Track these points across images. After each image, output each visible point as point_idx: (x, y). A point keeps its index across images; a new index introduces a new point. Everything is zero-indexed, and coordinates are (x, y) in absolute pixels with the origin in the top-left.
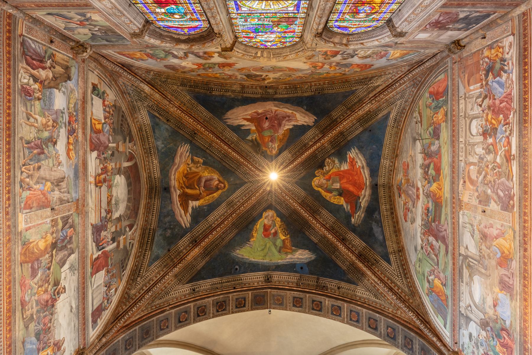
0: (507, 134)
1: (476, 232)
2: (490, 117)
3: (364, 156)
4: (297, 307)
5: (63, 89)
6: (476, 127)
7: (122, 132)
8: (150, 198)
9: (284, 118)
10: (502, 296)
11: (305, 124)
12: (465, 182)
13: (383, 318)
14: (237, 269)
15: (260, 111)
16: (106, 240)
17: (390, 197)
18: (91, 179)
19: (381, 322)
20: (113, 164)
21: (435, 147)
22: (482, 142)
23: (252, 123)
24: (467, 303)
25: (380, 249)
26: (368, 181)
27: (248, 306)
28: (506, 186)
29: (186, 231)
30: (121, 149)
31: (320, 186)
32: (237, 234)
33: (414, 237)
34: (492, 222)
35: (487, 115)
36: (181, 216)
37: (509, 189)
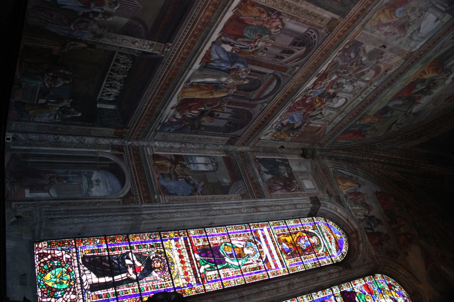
0: (311, 91)
2: (318, 105)
6: (337, 102)
12: (386, 71)
21: (396, 103)
22: (340, 92)
28: (342, 59)
34: (383, 36)
35: (319, 107)
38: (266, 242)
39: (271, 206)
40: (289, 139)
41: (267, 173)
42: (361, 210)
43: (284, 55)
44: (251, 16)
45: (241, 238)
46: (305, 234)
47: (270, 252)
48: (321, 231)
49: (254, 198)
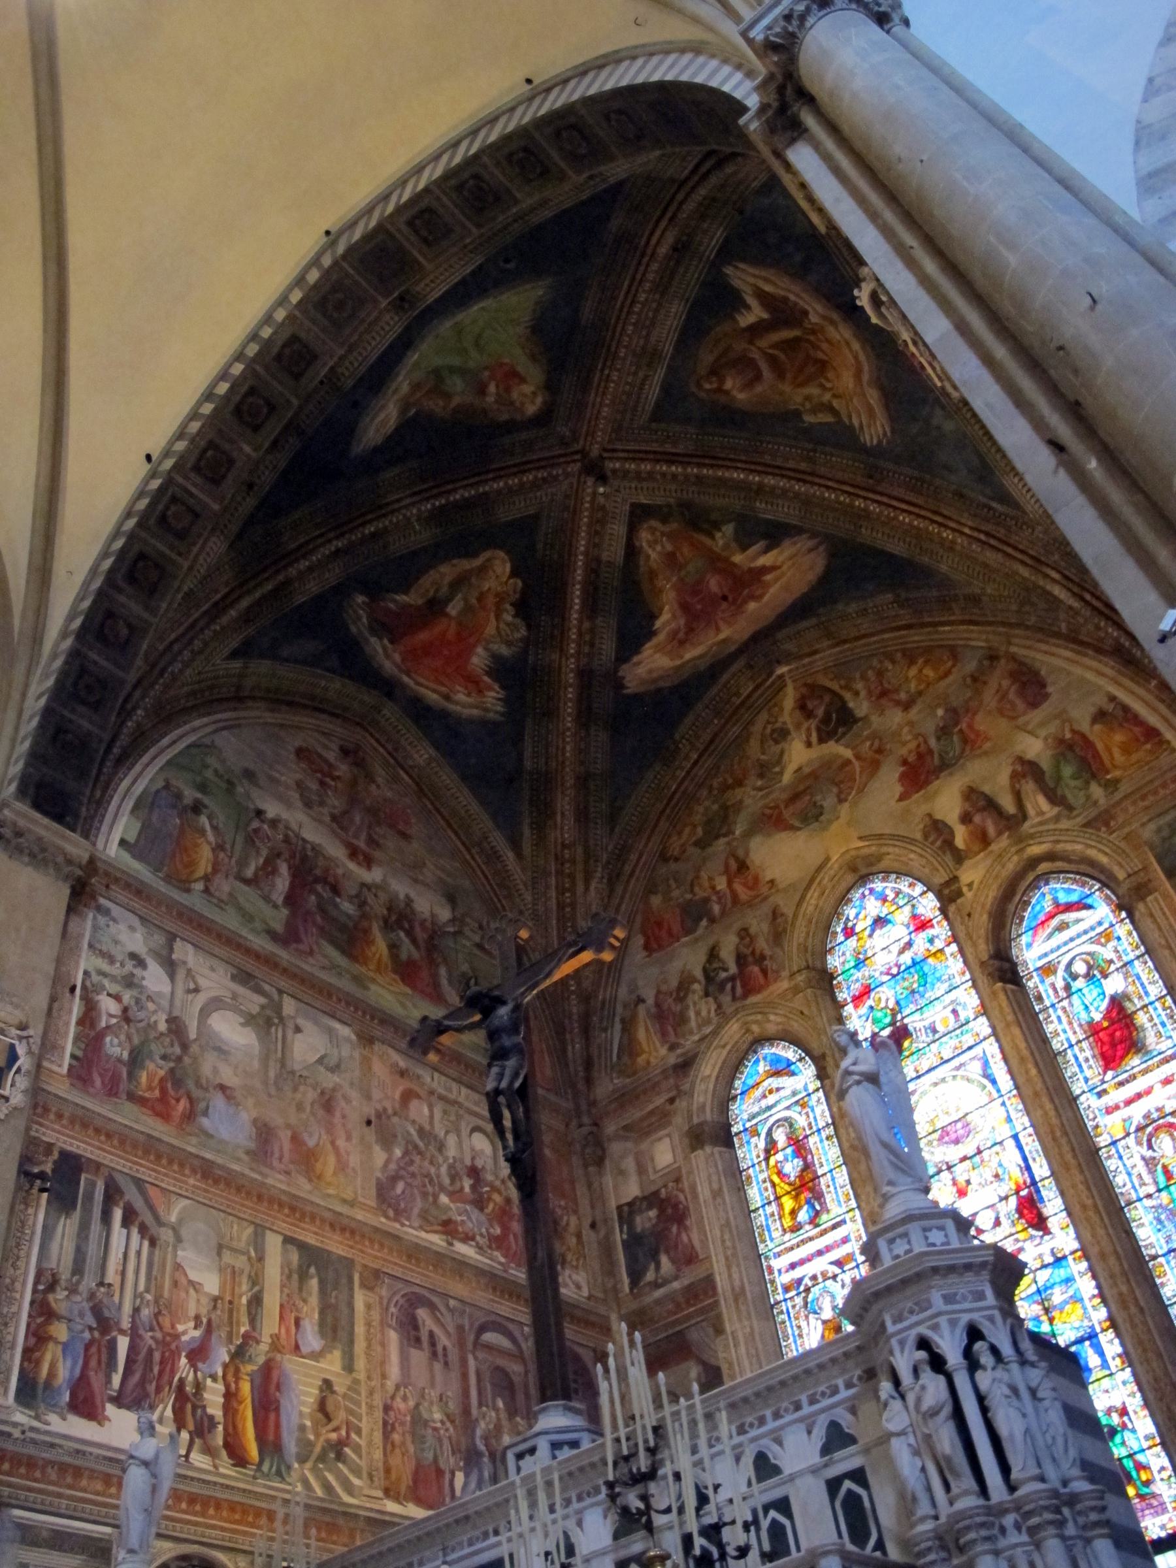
3: (471, 721)
4: (284, 346)
9: (690, 630)
11: (635, 659)
14: (507, 261)
15: (752, 606)
19: (147, 608)
23: (751, 570)
24: (202, 982)
26: (411, 683)
27: (399, 230)
29: (727, 253)
31: (482, 570)
36: (766, 280)
38: (802, 1262)
39: (727, 1259)
40: (573, 1220)
41: (658, 1267)
42: (695, 1004)
45: (803, 1324)
46: (772, 1161)
47: (820, 1253)
48: (758, 1114)
49: (716, 1303)
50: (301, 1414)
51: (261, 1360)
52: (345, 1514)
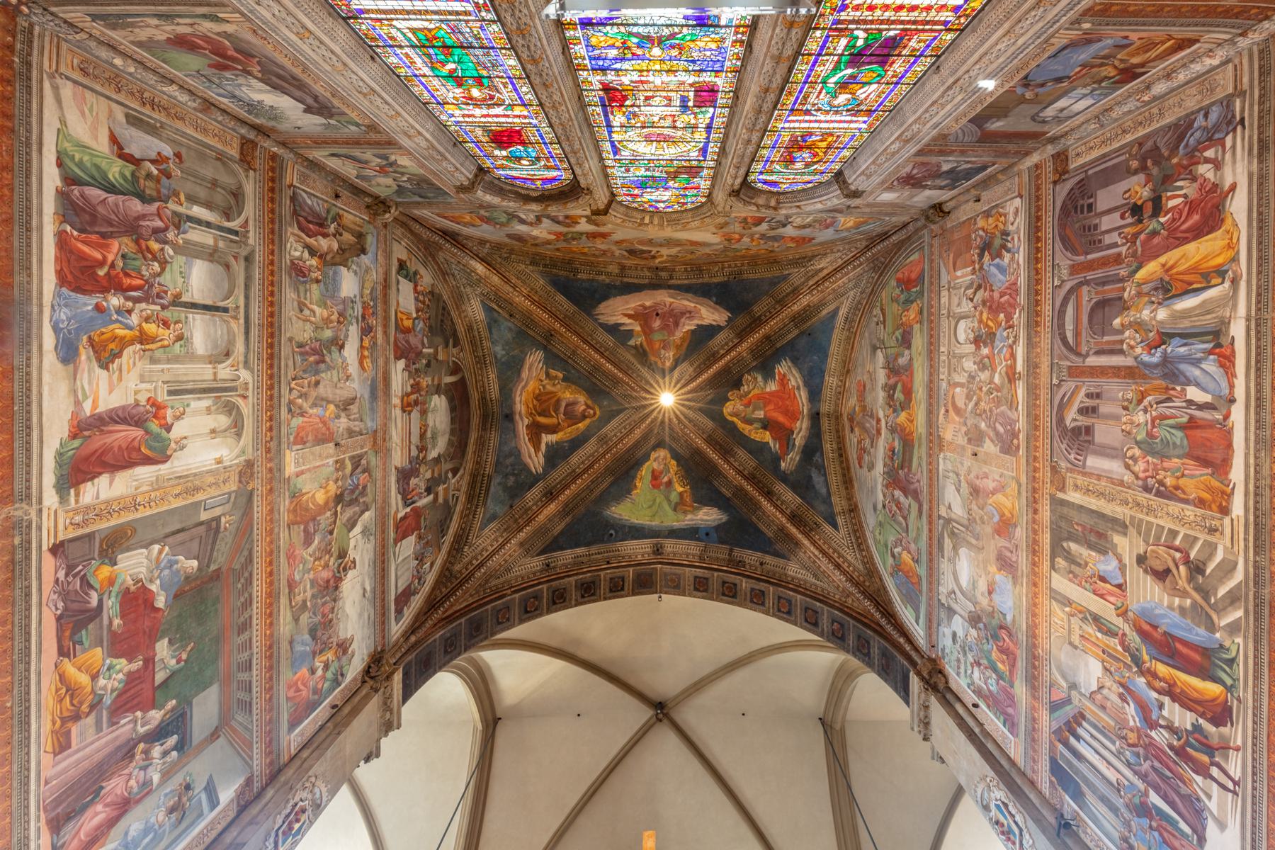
1: (964, 484)
3: (800, 370)
5: (354, 267)
7: (443, 331)
8: (484, 429)
10: (1001, 578)
12: (947, 411)
13: (826, 608)
16: (417, 491)
17: (838, 431)
18: (396, 401)
20: (429, 379)
25: (822, 508)
29: (536, 479)
30: (440, 357)
31: (736, 415)
32: (612, 484)
33: (873, 491)
37: (1013, 422)
43: (1090, 403)
44: (1192, 476)
50: (1171, 607)
51: (1138, 639)
52: (1256, 584)
